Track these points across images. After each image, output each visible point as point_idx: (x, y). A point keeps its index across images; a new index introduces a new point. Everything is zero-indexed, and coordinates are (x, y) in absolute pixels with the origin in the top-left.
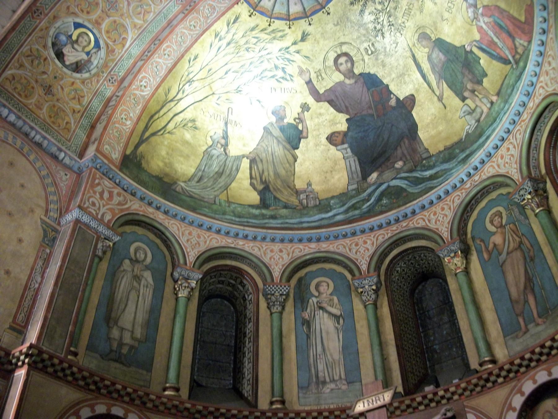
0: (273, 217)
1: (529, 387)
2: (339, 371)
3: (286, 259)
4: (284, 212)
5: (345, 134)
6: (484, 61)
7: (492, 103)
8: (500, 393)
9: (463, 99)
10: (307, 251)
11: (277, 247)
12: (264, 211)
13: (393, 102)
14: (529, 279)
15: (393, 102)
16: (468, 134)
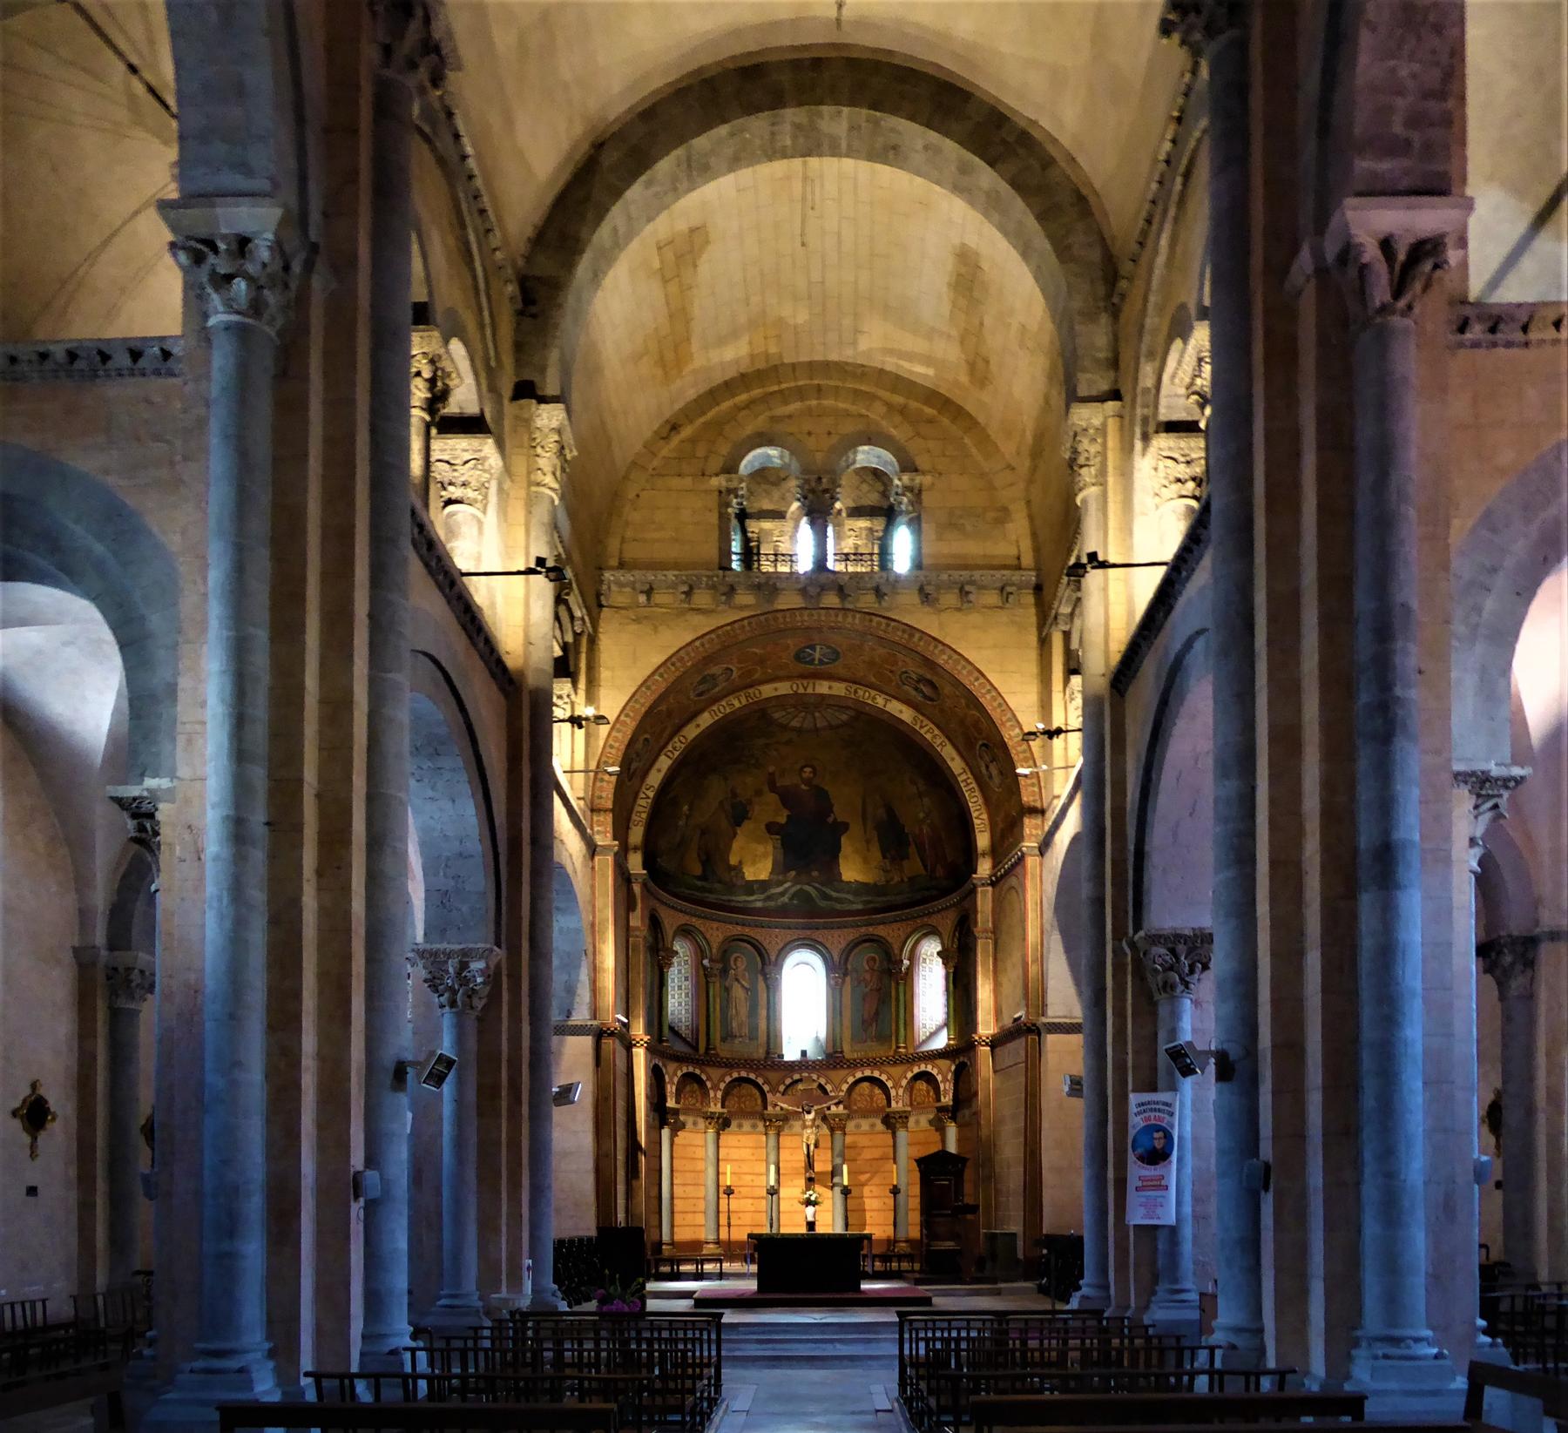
0: (710, 891)
1: (859, 1075)
2: (746, 1031)
3: (721, 938)
4: (717, 886)
5: (782, 826)
6: (912, 850)
7: (902, 881)
8: (843, 1073)
9: (884, 857)
10: (735, 932)
11: (715, 925)
12: (704, 883)
13: (830, 820)
14: (877, 1013)
15: (830, 820)
16: (875, 885)
